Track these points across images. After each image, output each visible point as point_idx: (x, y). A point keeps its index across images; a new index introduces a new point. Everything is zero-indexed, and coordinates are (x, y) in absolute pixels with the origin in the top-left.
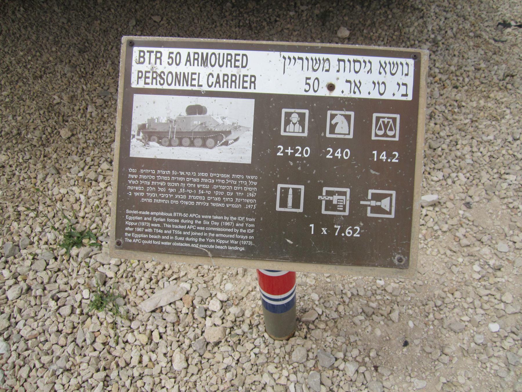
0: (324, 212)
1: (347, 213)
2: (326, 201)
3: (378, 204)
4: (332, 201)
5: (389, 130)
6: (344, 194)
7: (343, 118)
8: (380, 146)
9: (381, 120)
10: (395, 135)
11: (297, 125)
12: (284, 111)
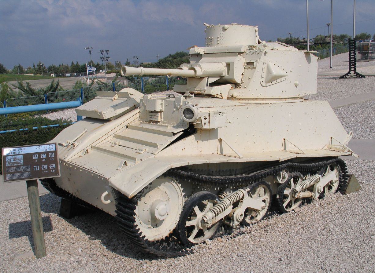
8: (51, 158)
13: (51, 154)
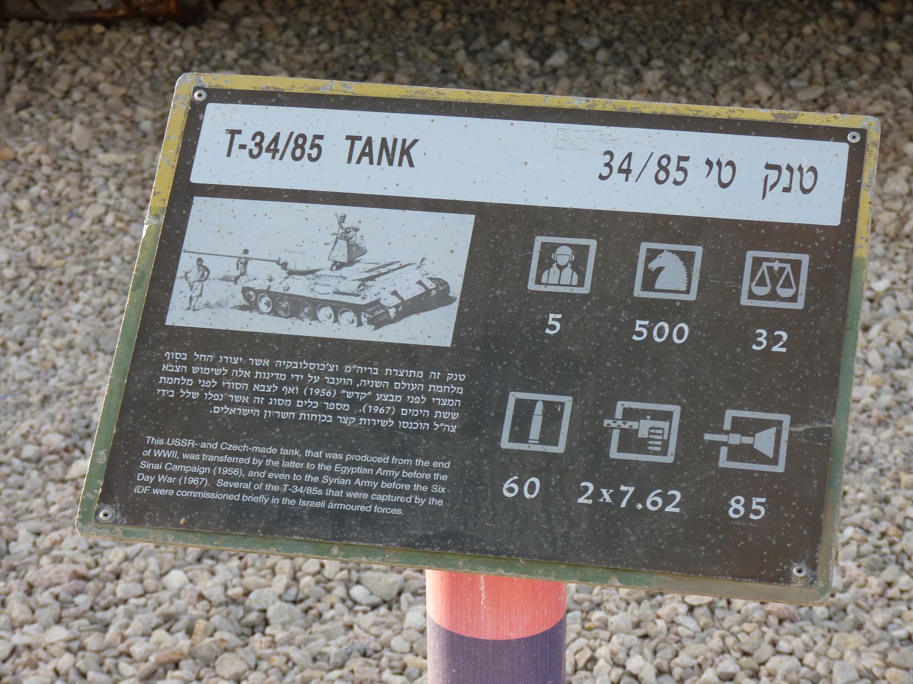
0: (614, 454)
1: (669, 459)
2: (623, 432)
3: (747, 440)
4: (637, 431)
5: (782, 286)
6: (667, 416)
7: (675, 258)
9: (765, 264)
10: (795, 298)
11: (568, 271)
12: (539, 240)
13: (776, 258)
